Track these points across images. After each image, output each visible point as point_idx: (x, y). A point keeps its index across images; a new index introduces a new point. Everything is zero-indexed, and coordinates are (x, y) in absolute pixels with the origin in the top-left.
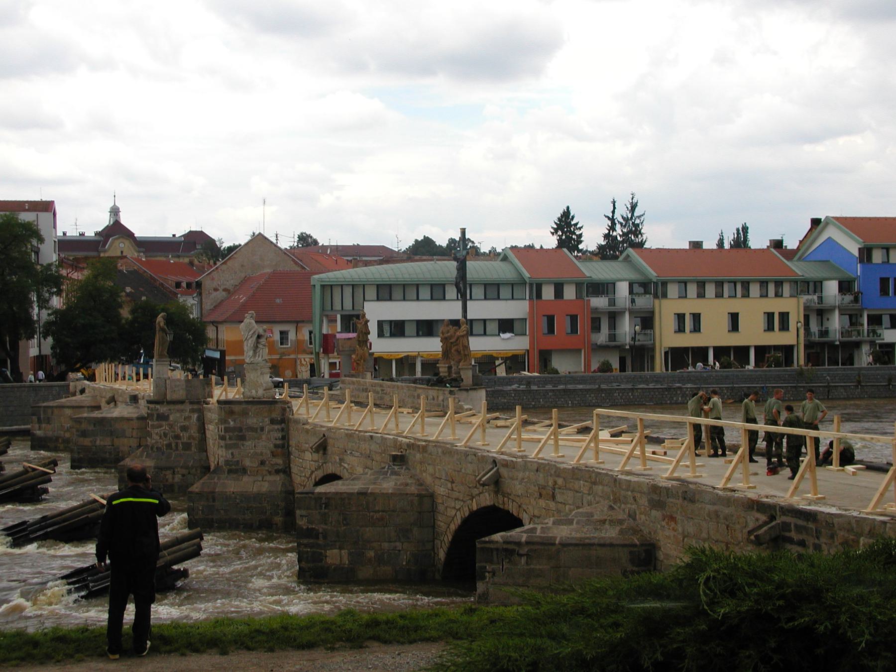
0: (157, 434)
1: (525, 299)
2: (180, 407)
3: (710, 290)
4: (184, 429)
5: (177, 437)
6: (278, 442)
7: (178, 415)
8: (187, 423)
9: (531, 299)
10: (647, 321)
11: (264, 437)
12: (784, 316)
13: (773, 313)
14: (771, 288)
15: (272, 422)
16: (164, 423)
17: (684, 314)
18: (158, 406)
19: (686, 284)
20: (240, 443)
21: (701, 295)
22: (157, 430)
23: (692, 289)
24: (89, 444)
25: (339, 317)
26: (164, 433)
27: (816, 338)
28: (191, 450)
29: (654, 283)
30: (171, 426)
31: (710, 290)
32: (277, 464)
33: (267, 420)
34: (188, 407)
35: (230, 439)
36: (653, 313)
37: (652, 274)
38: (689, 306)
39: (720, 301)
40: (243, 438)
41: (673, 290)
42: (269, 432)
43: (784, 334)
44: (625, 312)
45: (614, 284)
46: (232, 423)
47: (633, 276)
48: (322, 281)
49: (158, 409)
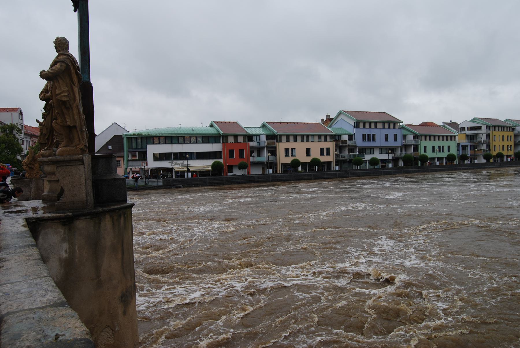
1: (221, 143)
3: (299, 138)
9: (223, 142)
10: (273, 152)
12: (328, 149)
13: (324, 148)
14: (323, 138)
17: (289, 149)
21: (295, 140)
23: (292, 138)
25: (137, 152)
27: (340, 158)
29: (276, 135)
31: (299, 138)
36: (276, 148)
37: (276, 132)
38: (290, 145)
39: (302, 143)
41: (284, 139)
43: (328, 157)
44: (264, 148)
45: (259, 136)
47: (268, 133)
48: (127, 136)
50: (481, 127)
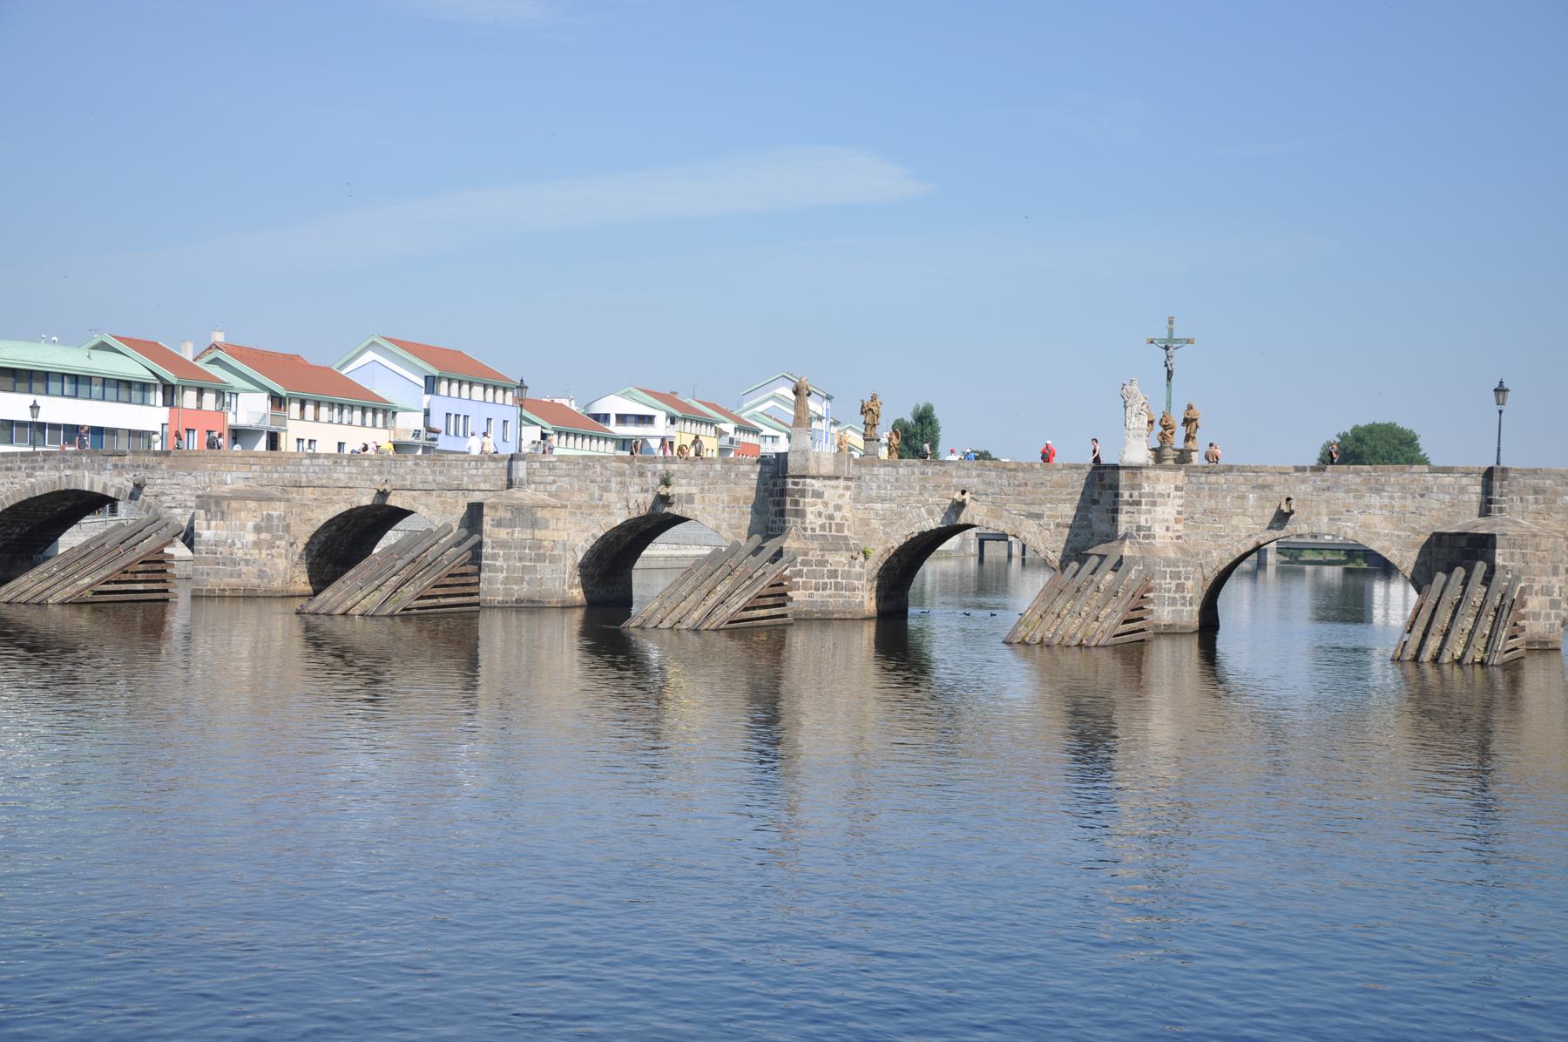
0: (812, 513)
2: (833, 483)
4: (838, 508)
5: (831, 517)
6: (1180, 509)
7: (832, 492)
8: (840, 502)
11: (1169, 503)
15: (1177, 489)
16: (819, 501)
18: (813, 481)
19: (470, 399)
20: (1153, 508)
22: (812, 509)
24: (506, 537)
26: (819, 512)
28: (843, 532)
30: (826, 504)
32: (1177, 531)
33: (1173, 486)
34: (842, 483)
35: (1146, 504)
40: (1154, 504)
42: (1174, 498)
46: (1147, 488)
49: (813, 485)
50: (654, 417)
